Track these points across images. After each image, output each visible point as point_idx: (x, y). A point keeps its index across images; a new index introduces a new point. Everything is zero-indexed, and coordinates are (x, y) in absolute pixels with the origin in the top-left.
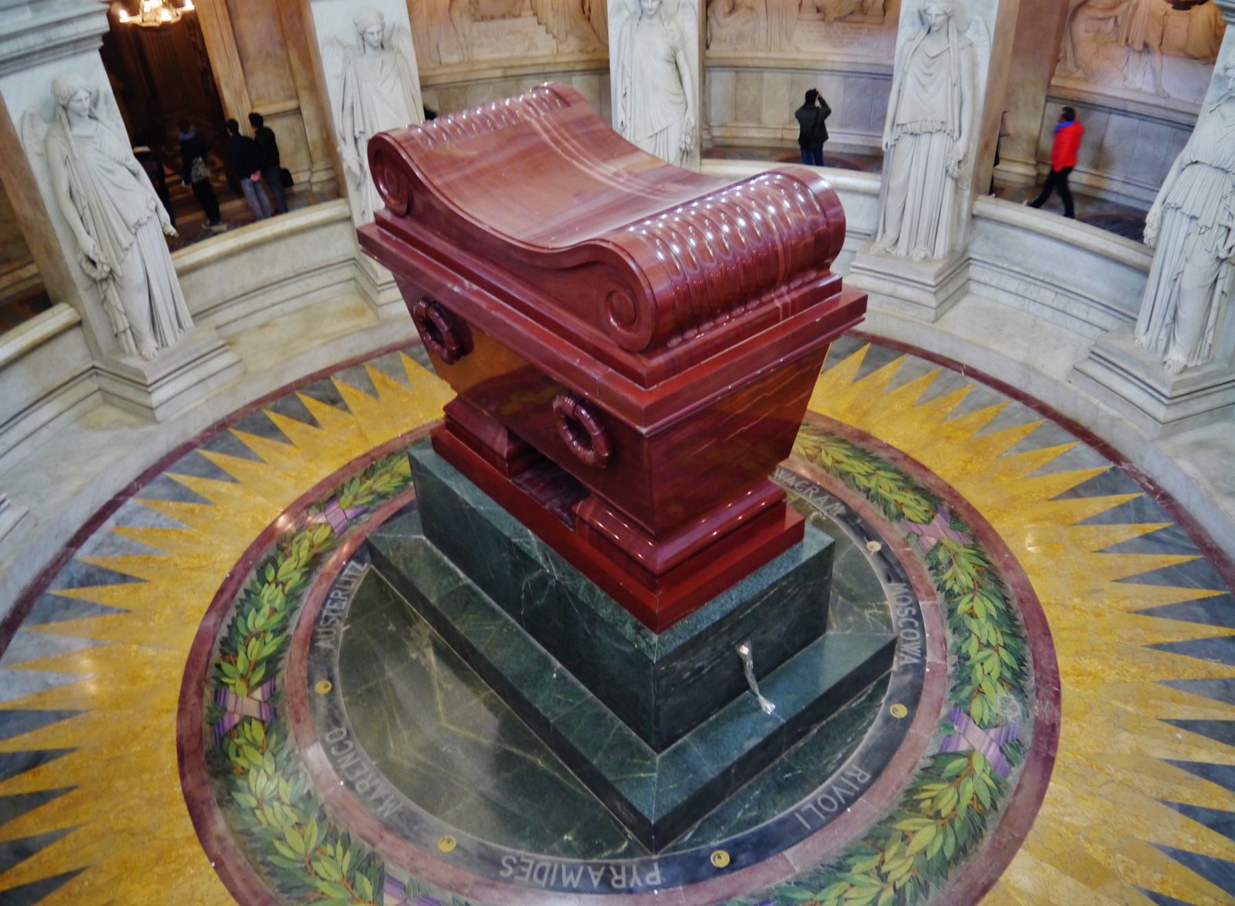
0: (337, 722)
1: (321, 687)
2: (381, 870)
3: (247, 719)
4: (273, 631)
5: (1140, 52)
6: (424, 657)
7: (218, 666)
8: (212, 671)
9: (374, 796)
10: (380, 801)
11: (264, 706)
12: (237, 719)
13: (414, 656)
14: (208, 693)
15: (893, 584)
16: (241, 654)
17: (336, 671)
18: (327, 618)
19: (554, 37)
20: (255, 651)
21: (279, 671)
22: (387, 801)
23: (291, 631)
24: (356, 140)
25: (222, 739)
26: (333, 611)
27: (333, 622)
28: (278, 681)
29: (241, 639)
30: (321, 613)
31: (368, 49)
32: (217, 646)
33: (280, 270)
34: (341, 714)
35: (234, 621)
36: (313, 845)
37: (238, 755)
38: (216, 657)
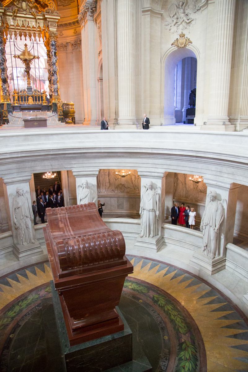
0: (163, 329)
1: (166, 338)
2: (153, 300)
3: (185, 334)
4: (182, 360)
6: (139, 339)
7: (196, 352)
8: (198, 350)
9: (154, 311)
10: (153, 310)
11: (181, 337)
12: (187, 335)
13: (142, 341)
14: (197, 344)
15: (20, 324)
16: (191, 354)
17: (162, 341)
18: (166, 359)
20: (187, 354)
21: (178, 346)
22: (151, 310)
23: (177, 358)
25: (189, 331)
26: (164, 362)
27: (164, 357)
28: (178, 343)
29: (192, 359)
30: (168, 362)
32: (199, 358)
34: (161, 330)
35: (196, 368)
37: (185, 326)
38: (198, 355)
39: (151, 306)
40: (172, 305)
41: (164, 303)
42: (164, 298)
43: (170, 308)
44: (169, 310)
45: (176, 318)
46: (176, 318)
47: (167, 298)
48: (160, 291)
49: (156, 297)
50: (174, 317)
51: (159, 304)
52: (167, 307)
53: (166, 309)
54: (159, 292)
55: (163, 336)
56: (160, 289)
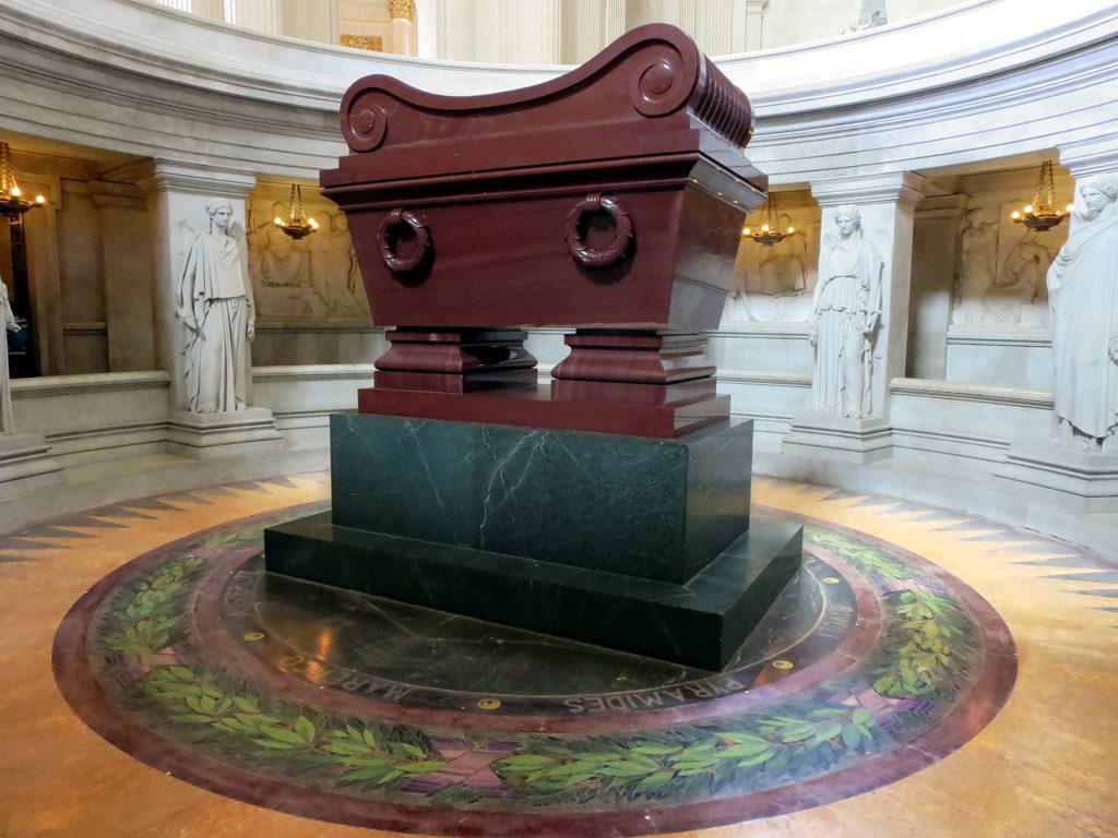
5: (735, 298)
10: (380, 692)
19: (326, 304)
24: (193, 301)
31: (215, 230)
33: (96, 421)
36: (312, 734)
39: (412, 705)
40: (268, 754)
41: (337, 747)
42: (353, 777)
43: (279, 733)
44: (283, 725)
45: (217, 706)
46: (217, 706)
47: (331, 782)
48: (420, 812)
49: (411, 758)
50: (233, 705)
51: (362, 731)
52: (304, 733)
53: (302, 722)
54: (422, 800)
55: (267, 637)
56: (426, 824)
